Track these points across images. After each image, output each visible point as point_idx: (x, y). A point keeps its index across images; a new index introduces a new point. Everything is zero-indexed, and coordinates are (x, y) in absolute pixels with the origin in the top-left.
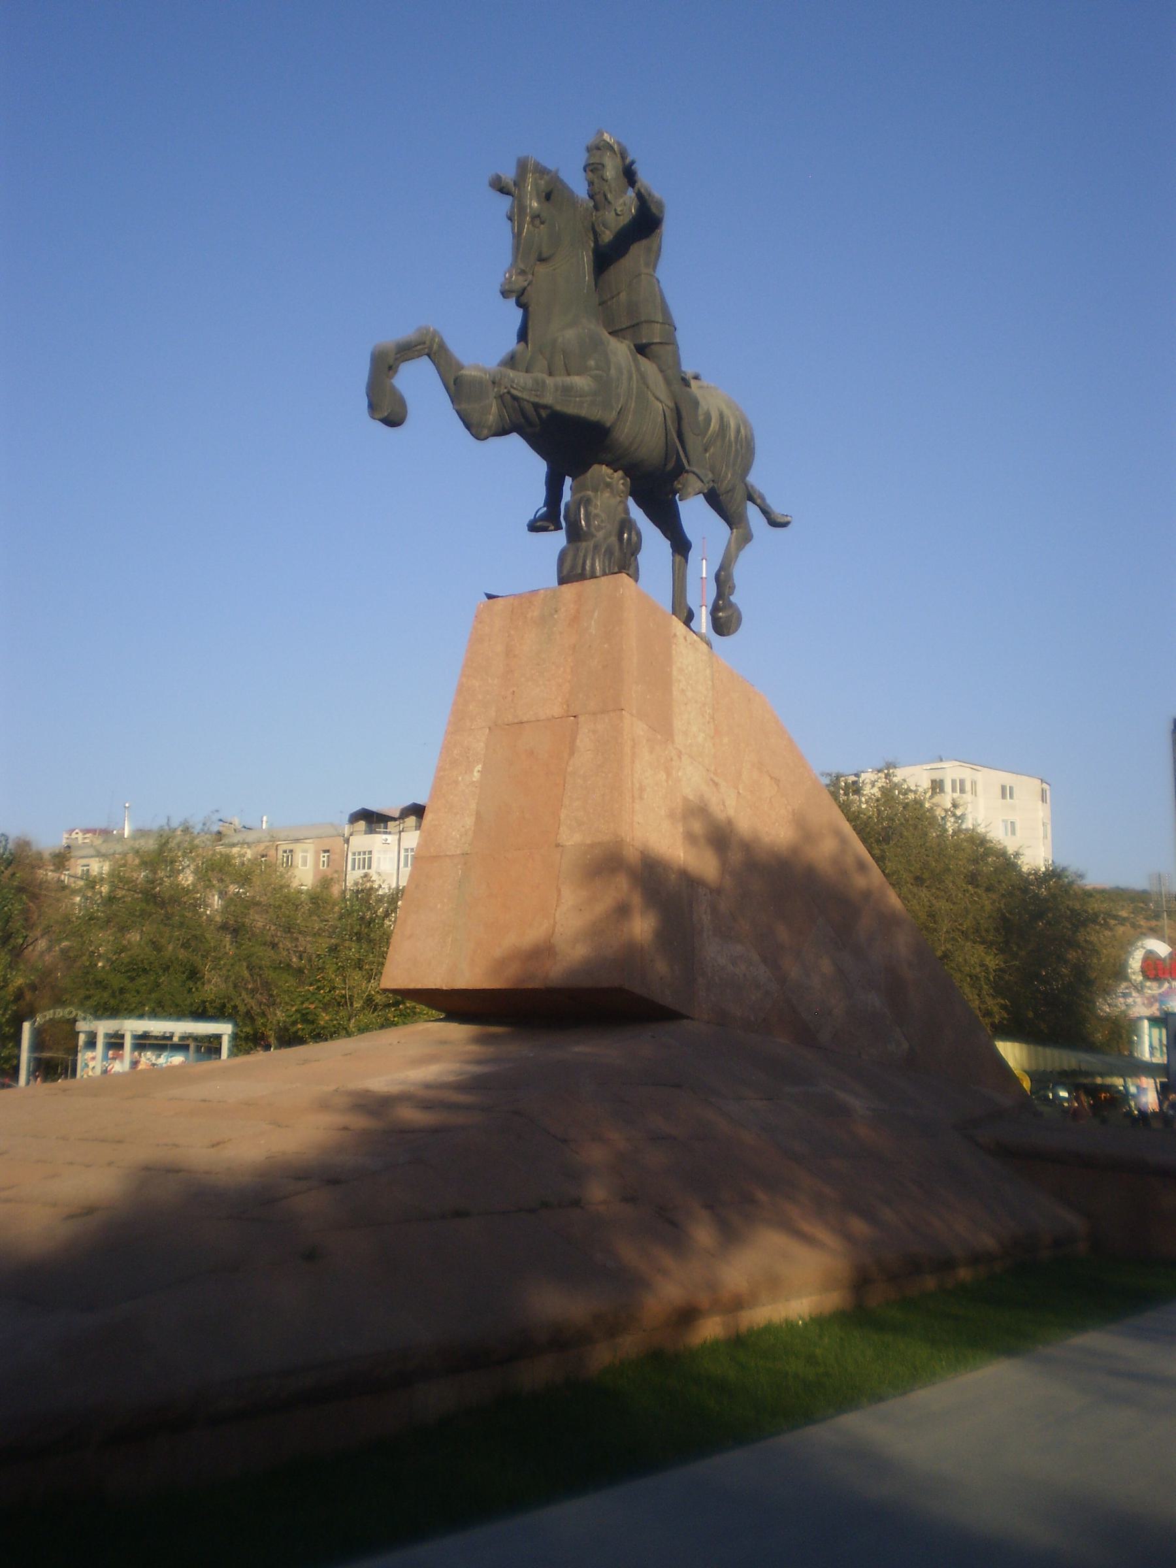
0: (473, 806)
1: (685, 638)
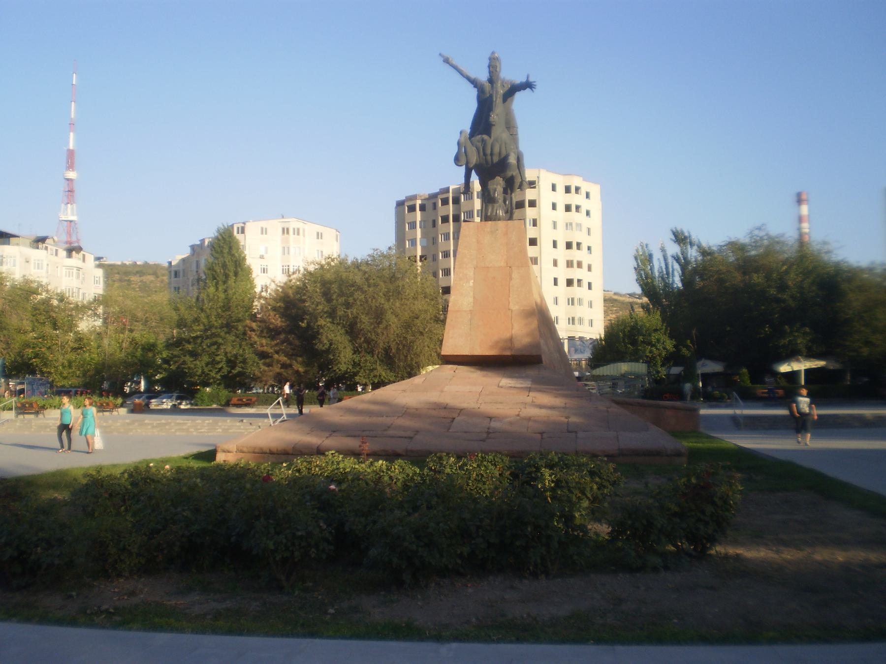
0: (472, 294)
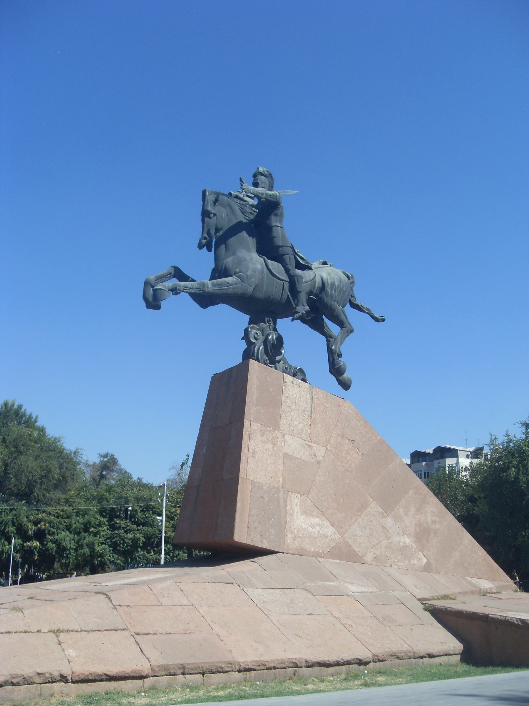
1: (292, 383)
